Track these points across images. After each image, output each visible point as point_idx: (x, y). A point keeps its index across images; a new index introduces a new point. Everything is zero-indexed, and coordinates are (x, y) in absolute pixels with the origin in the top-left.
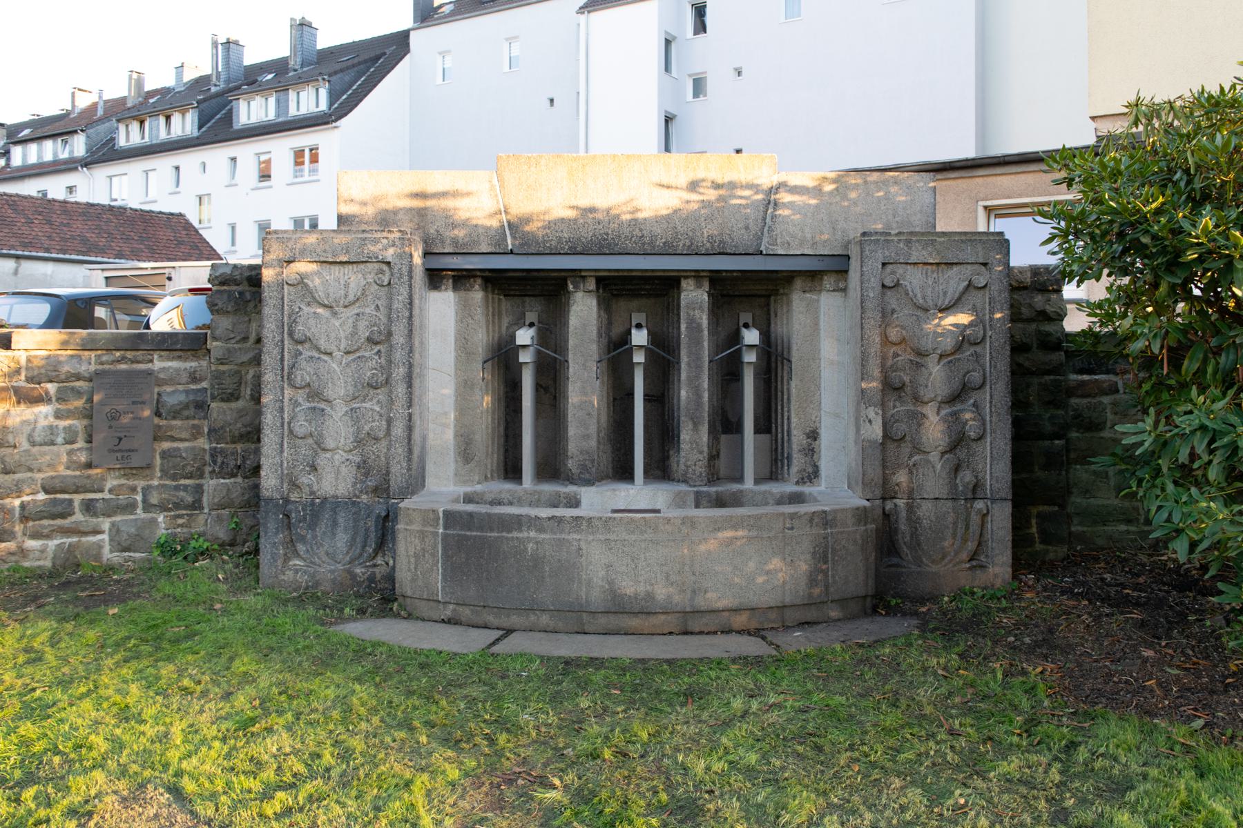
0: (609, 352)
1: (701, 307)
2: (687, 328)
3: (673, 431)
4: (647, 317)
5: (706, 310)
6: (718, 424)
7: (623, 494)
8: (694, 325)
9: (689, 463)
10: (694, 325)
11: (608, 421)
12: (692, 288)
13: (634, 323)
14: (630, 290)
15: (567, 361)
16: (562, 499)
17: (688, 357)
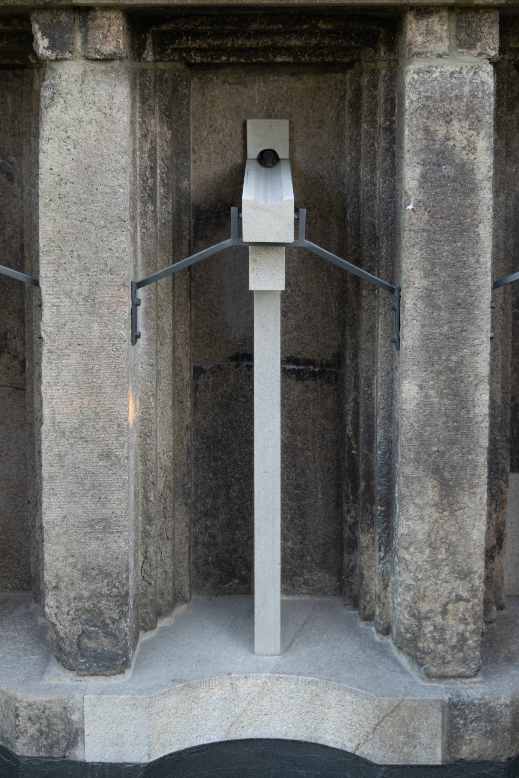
0: (177, 256)
1: (470, 110)
2: (424, 178)
3: (369, 476)
4: (292, 129)
5: (489, 119)
6: (504, 453)
7: (217, 692)
8: (447, 170)
9: (424, 607)
10: (447, 170)
11: (178, 441)
12: (443, 47)
13: (253, 152)
14: (241, 51)
15: (36, 283)
16: (22, 722)
17: (427, 275)
